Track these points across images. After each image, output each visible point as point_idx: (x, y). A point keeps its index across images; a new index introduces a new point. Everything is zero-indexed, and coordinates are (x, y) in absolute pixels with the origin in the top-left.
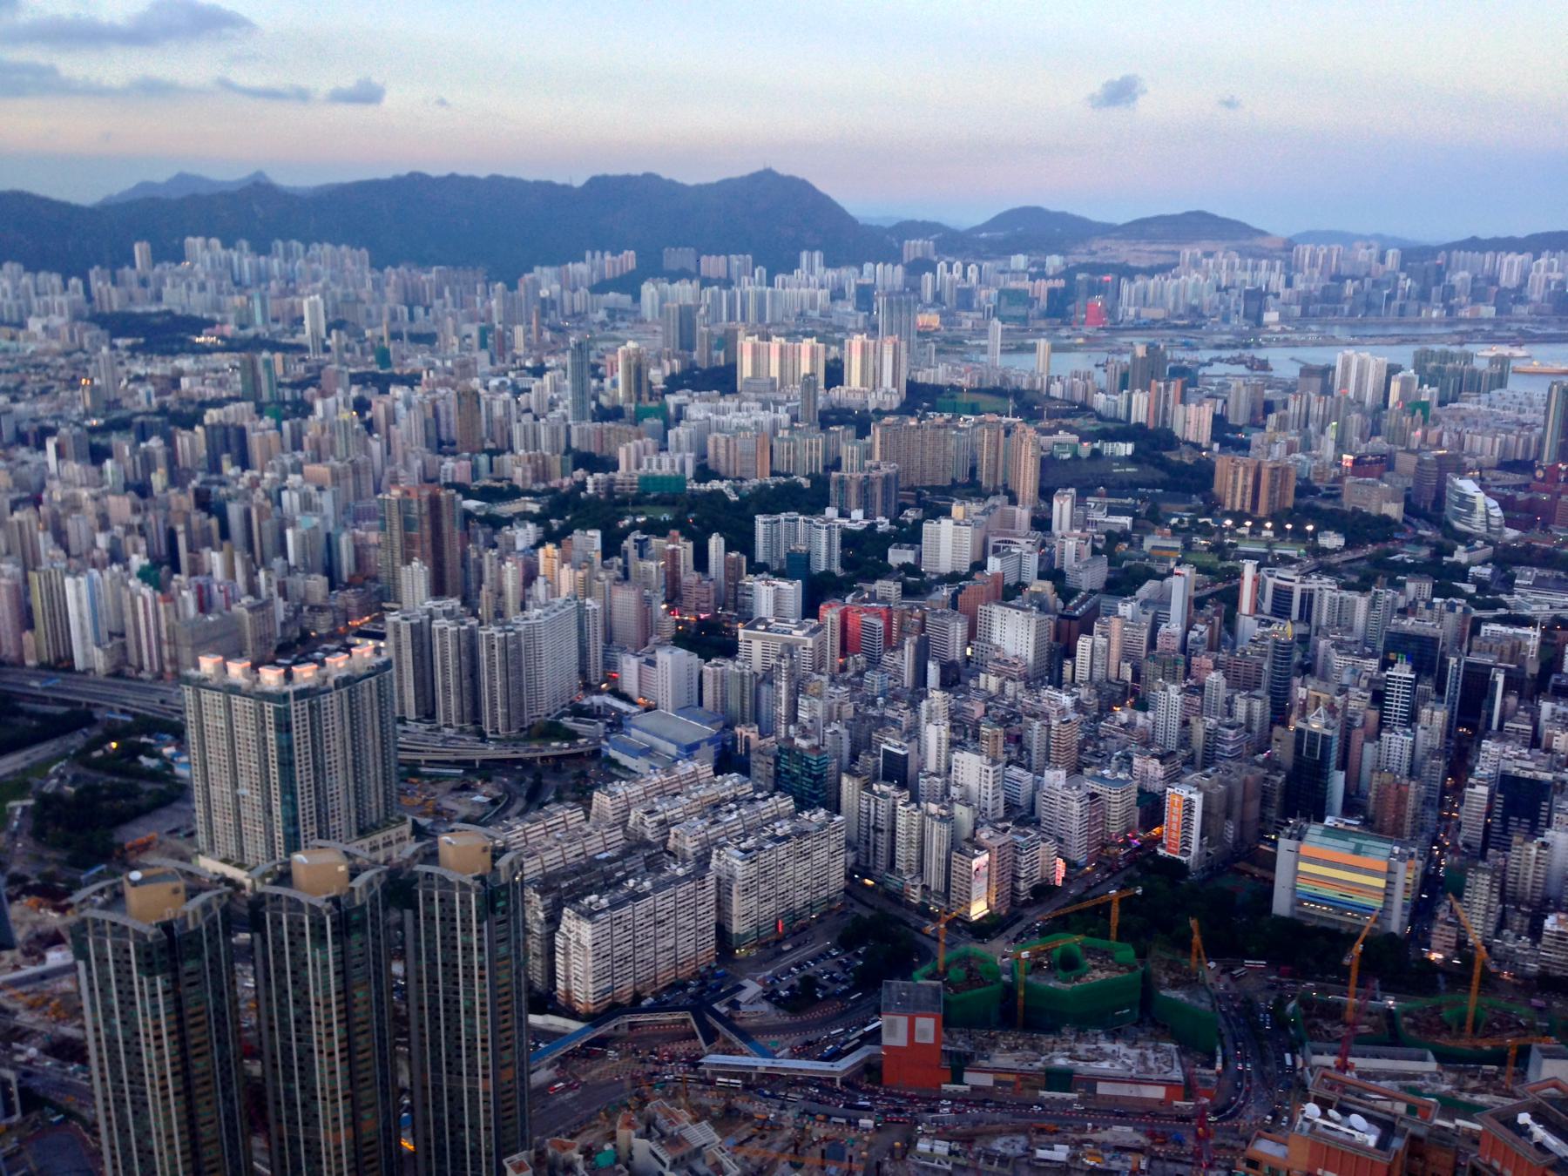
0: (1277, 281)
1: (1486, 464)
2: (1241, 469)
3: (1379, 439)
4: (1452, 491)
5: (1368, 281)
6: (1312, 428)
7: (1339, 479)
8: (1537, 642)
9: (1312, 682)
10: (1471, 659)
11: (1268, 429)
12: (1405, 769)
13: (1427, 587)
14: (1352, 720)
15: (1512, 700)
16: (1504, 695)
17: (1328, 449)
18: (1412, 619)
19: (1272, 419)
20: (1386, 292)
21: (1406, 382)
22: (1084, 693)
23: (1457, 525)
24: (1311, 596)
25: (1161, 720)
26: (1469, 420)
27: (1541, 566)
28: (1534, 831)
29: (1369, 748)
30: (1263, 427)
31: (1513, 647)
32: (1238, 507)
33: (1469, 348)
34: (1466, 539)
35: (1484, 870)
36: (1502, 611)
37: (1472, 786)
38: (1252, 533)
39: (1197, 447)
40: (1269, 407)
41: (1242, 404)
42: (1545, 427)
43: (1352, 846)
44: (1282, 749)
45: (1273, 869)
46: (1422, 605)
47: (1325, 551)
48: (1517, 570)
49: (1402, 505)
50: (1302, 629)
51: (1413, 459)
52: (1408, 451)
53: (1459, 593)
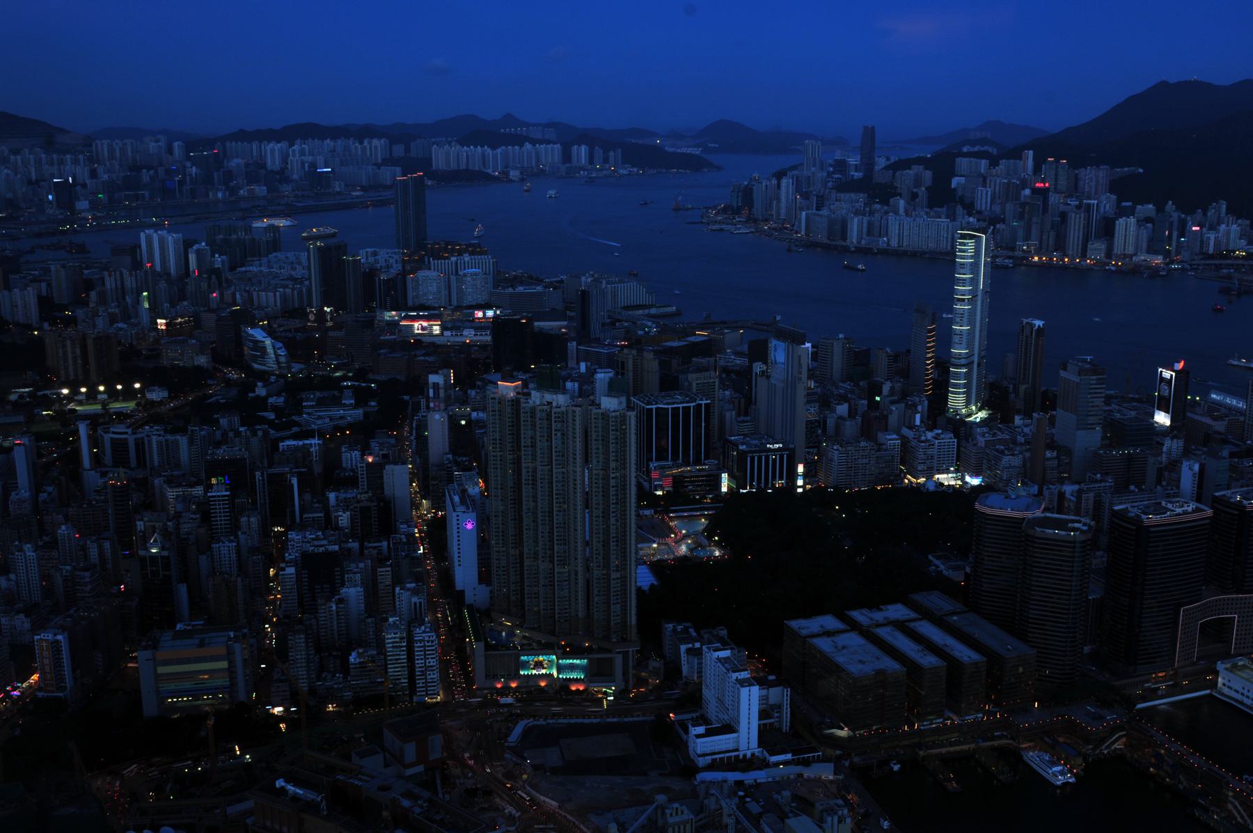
0: (83, 172)
2: (68, 342)
3: (185, 303)
5: (161, 171)
6: (128, 299)
7: (157, 341)
8: (317, 448)
13: (236, 419)
15: (308, 497)
16: (300, 495)
18: (224, 447)
19: (93, 294)
20: (177, 179)
21: (198, 252)
23: (256, 366)
24: (143, 443)
28: (334, 591)
29: (203, 559)
30: (87, 305)
34: (263, 376)
36: (295, 429)
37: (283, 569)
40: (89, 285)
42: (309, 279)
43: (197, 641)
46: (231, 434)
47: (152, 403)
52: (210, 310)
53: (264, 420)
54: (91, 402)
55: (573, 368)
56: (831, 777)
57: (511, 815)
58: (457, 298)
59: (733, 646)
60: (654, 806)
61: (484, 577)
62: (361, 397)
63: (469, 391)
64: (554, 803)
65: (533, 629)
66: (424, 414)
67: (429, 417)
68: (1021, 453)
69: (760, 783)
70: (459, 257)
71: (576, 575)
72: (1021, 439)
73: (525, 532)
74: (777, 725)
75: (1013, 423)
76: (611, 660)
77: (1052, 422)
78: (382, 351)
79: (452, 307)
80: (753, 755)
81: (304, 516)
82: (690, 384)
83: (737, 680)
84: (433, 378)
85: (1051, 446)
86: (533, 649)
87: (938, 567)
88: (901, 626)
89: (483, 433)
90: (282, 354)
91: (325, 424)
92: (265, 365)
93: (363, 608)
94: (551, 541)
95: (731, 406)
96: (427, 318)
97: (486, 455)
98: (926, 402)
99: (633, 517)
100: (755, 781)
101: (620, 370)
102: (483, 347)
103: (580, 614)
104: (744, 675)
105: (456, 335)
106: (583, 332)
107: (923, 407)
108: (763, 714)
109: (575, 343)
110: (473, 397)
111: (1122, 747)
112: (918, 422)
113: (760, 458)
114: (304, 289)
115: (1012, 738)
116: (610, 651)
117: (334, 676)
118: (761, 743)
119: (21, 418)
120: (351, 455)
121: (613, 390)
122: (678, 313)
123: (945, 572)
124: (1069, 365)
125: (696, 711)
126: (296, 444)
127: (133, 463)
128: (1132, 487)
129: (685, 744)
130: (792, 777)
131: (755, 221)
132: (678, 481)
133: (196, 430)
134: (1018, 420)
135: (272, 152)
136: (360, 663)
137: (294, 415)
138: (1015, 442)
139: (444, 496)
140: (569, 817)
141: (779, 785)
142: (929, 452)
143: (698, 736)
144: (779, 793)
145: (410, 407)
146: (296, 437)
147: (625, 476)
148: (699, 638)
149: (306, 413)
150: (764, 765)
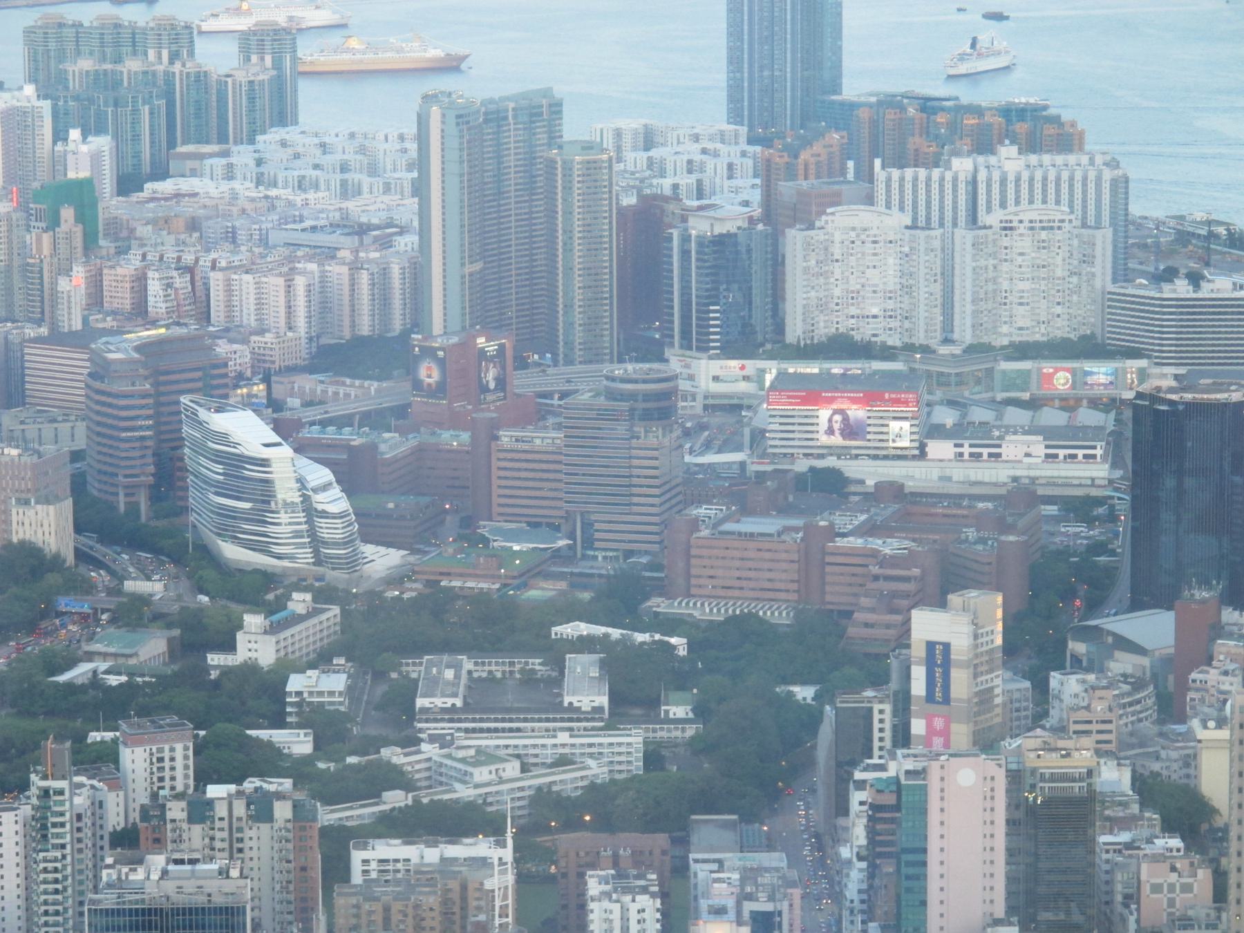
1: (278, 360)
4: (200, 449)
8: (510, 878)
23: (231, 552)
26: (213, 228)
31: (446, 902)
36: (395, 799)
46: (176, 811)
48: (415, 669)
49: (69, 502)
51: (77, 363)
52: (58, 338)
58: (976, 313)
63: (1055, 678)
66: (909, 765)
70: (981, 159)
78: (702, 511)
79: (957, 350)
89: (1129, 846)
90: (333, 509)
91: (501, 781)
92: (263, 549)
96: (872, 392)
105: (976, 457)
110: (1068, 700)
114: (396, 270)
120: (625, 910)
126: (415, 860)
133: (61, 792)
137: (387, 743)
145: (826, 732)
149: (433, 739)
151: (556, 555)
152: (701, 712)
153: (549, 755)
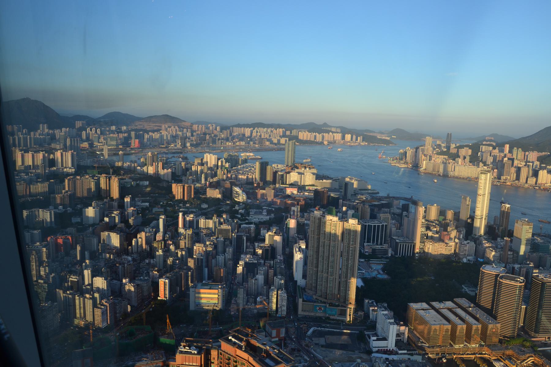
0: (189, 134)
2: (179, 187)
5: (213, 135)
9: (197, 245)
10: (238, 234)
11: (187, 176)
12: (223, 265)
13: (228, 216)
14: (209, 254)
15: (249, 244)
16: (246, 243)
17: (203, 181)
20: (217, 138)
21: (222, 162)
22: (135, 256)
23: (236, 199)
25: (158, 260)
27: (256, 209)
29: (213, 261)
30: (186, 176)
32: (179, 198)
33: (239, 153)
35: (242, 288)
36: (247, 221)
37: (238, 267)
38: (183, 205)
39: (168, 182)
41: (180, 169)
43: (209, 287)
44: (191, 263)
45: (189, 298)
46: (226, 221)
50: (196, 231)
54: (184, 207)
55: (340, 209)
56: (421, 361)
57: (306, 359)
59: (389, 310)
60: (356, 363)
61: (304, 276)
62: (269, 212)
63: (305, 214)
64: (321, 357)
65: (319, 296)
67: (290, 222)
68: (499, 251)
69: (394, 360)
71: (336, 279)
72: (499, 246)
73: (319, 263)
74: (402, 340)
75: (497, 240)
76: (346, 311)
77: (511, 241)
80: (393, 349)
81: (247, 250)
82: (380, 217)
83: (389, 322)
84: (293, 208)
85: (511, 250)
86: (318, 303)
87: (465, 290)
88: (450, 310)
92: (239, 199)
93: (263, 282)
94: (328, 267)
95: (394, 226)
97: (308, 235)
98: (465, 231)
99: (357, 262)
100: (393, 359)
101: (356, 211)
102: (311, 199)
103: (336, 293)
104: (392, 321)
106: (345, 198)
107: (464, 231)
108: (398, 335)
109: (341, 200)
111: (531, 363)
112: (461, 237)
113: (403, 245)
115: (489, 355)
116: (345, 307)
117: (251, 304)
118: (396, 345)
119: (163, 210)
121: (354, 217)
122: (378, 193)
123: (468, 292)
124: (519, 221)
125: (374, 331)
127: (195, 227)
128: (541, 268)
129: (369, 343)
130: (406, 359)
131: (407, 163)
132: (374, 250)
134: (499, 239)
135: (247, 132)
136: (260, 301)
138: (497, 247)
139: (293, 248)
140: (326, 363)
141: (401, 362)
142: (465, 248)
143: (374, 340)
144: (401, 364)
145: (285, 217)
146: (246, 224)
147: (355, 247)
148: (377, 306)
150: (397, 353)
151: (264, 201)
152: (274, 215)
153: (261, 218)
